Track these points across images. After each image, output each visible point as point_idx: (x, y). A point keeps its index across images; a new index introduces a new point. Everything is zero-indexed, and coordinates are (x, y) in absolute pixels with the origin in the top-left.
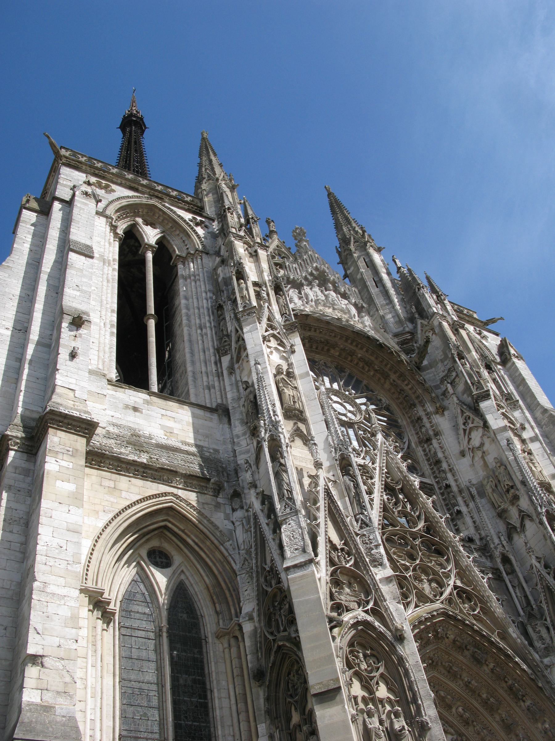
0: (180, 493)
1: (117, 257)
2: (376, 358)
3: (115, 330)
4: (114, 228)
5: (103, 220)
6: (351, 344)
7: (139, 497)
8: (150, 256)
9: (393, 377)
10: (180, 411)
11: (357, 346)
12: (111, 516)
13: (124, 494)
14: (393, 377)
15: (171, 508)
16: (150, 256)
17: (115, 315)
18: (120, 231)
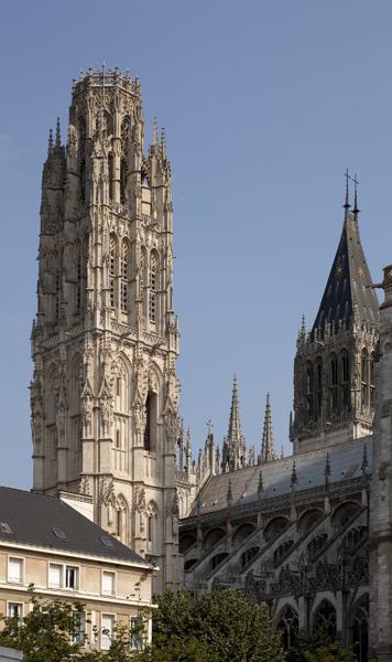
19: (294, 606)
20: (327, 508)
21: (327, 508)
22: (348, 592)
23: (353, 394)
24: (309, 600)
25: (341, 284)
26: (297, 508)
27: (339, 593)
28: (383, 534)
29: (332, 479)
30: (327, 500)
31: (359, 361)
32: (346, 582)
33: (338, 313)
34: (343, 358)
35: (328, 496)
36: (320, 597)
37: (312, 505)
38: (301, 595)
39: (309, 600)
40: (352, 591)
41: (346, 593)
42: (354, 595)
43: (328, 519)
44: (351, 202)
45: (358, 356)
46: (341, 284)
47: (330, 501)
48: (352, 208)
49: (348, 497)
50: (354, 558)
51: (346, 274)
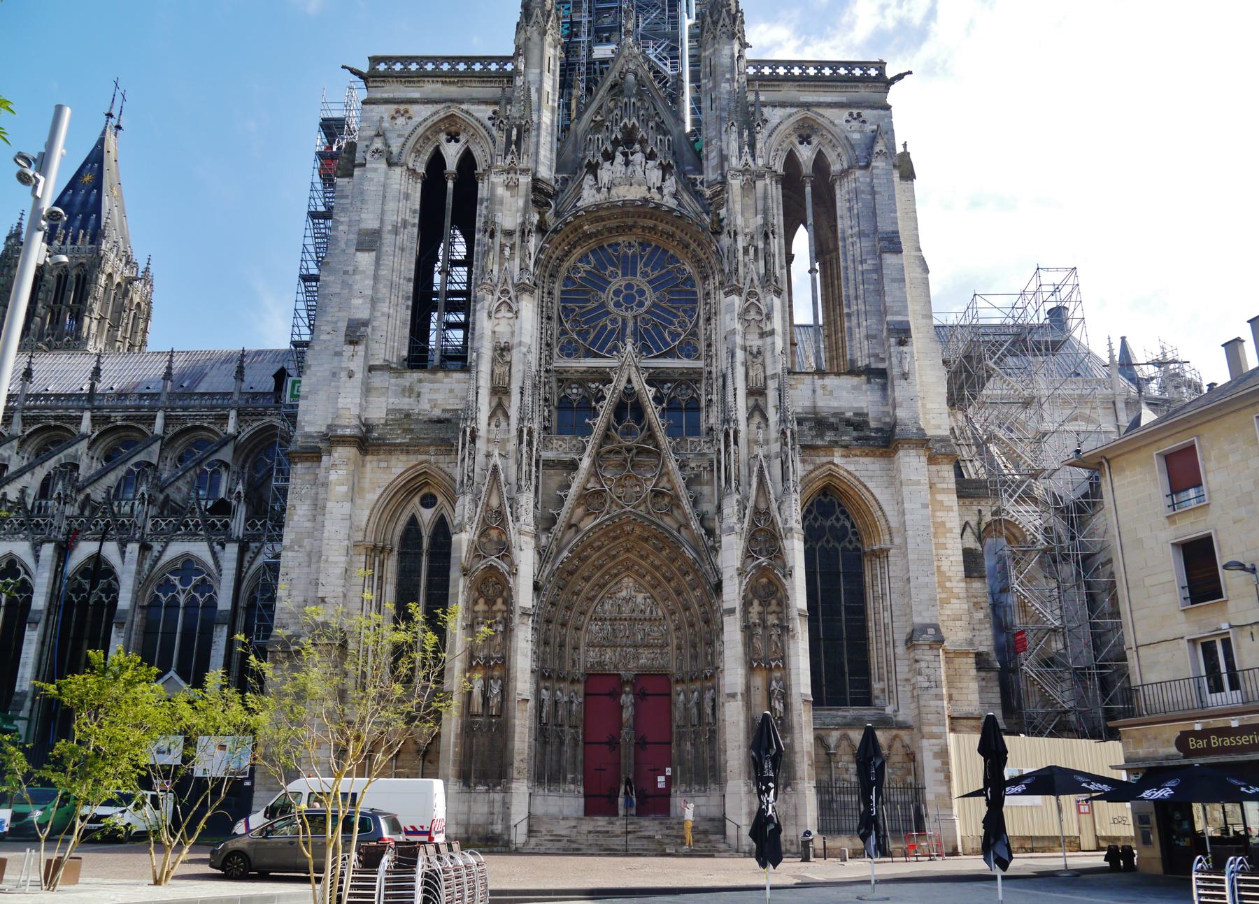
0: (432, 459)
1: (417, 206)
2: (677, 228)
3: (410, 303)
4: (413, 172)
5: (398, 170)
6: (651, 218)
7: (403, 470)
8: (450, 185)
9: (693, 246)
10: (446, 380)
11: (656, 220)
12: (383, 489)
13: (393, 470)
14: (693, 246)
15: (425, 472)
16: (450, 185)
17: (412, 284)
18: (421, 170)
19: (29, 561)
20: (86, 425)
21: (86, 425)
22: (149, 548)
23: (87, 320)
24: (64, 551)
25: (88, 193)
26: (24, 419)
27: (133, 548)
28: (348, 432)
29: (100, 387)
30: (87, 416)
31: (103, 284)
32: (148, 531)
33: (77, 223)
34: (78, 276)
35: (91, 409)
36: (85, 550)
37: (57, 418)
38: (50, 542)
39: (64, 551)
40: (157, 547)
41: (145, 548)
42: (161, 553)
43: (85, 443)
44: (115, 113)
45: (103, 279)
46: (88, 193)
47: (93, 419)
48: (113, 122)
49: (127, 418)
50: (162, 497)
51: (98, 184)
